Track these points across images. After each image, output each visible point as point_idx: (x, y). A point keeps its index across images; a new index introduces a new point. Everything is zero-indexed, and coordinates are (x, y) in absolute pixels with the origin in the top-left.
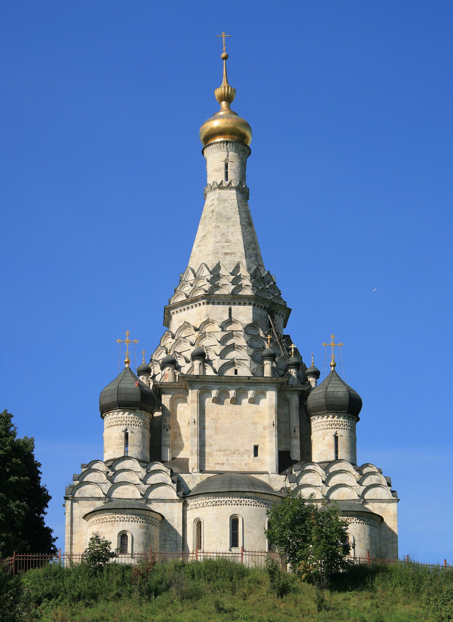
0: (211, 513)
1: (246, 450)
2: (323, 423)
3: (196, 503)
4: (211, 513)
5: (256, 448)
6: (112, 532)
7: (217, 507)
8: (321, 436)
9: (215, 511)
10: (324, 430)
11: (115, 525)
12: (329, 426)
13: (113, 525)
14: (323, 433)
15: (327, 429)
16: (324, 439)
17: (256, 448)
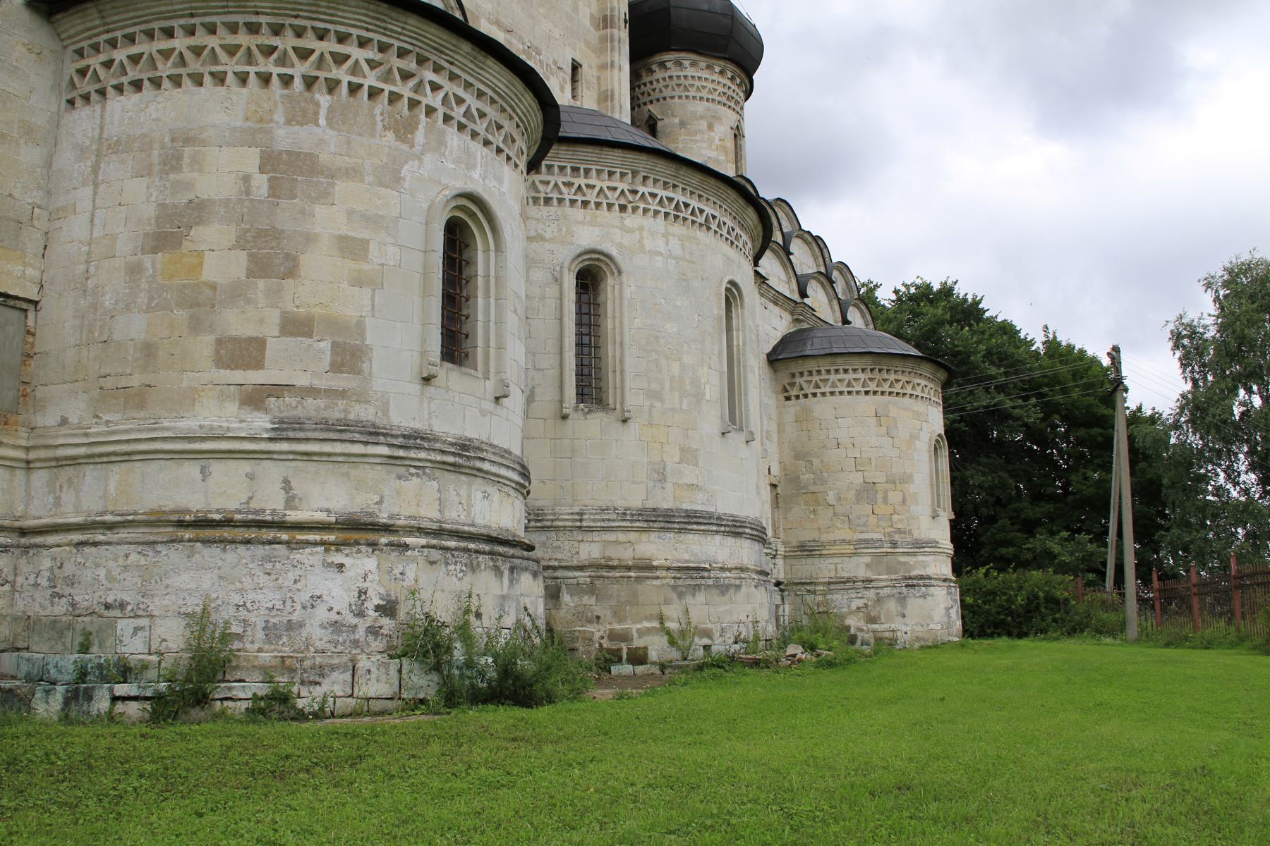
0: (660, 245)
1: (555, 62)
2: (711, 86)
3: (581, 181)
4: (660, 245)
5: (575, 67)
6: (391, 177)
7: (678, 229)
8: (702, 117)
9: (675, 245)
10: (710, 105)
11: (420, 136)
12: (724, 100)
13: (404, 131)
14: (709, 110)
15: (719, 102)
16: (710, 127)
17: (575, 67)
